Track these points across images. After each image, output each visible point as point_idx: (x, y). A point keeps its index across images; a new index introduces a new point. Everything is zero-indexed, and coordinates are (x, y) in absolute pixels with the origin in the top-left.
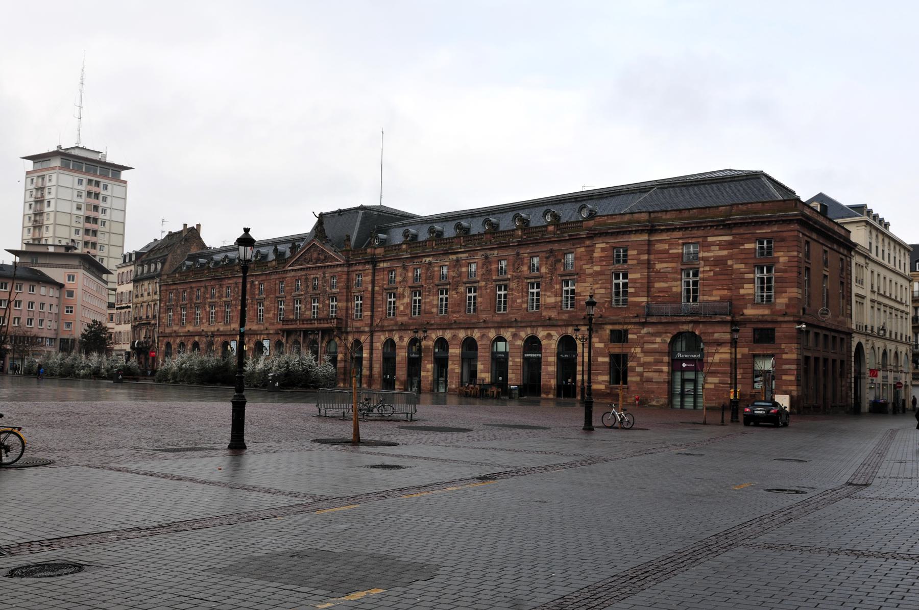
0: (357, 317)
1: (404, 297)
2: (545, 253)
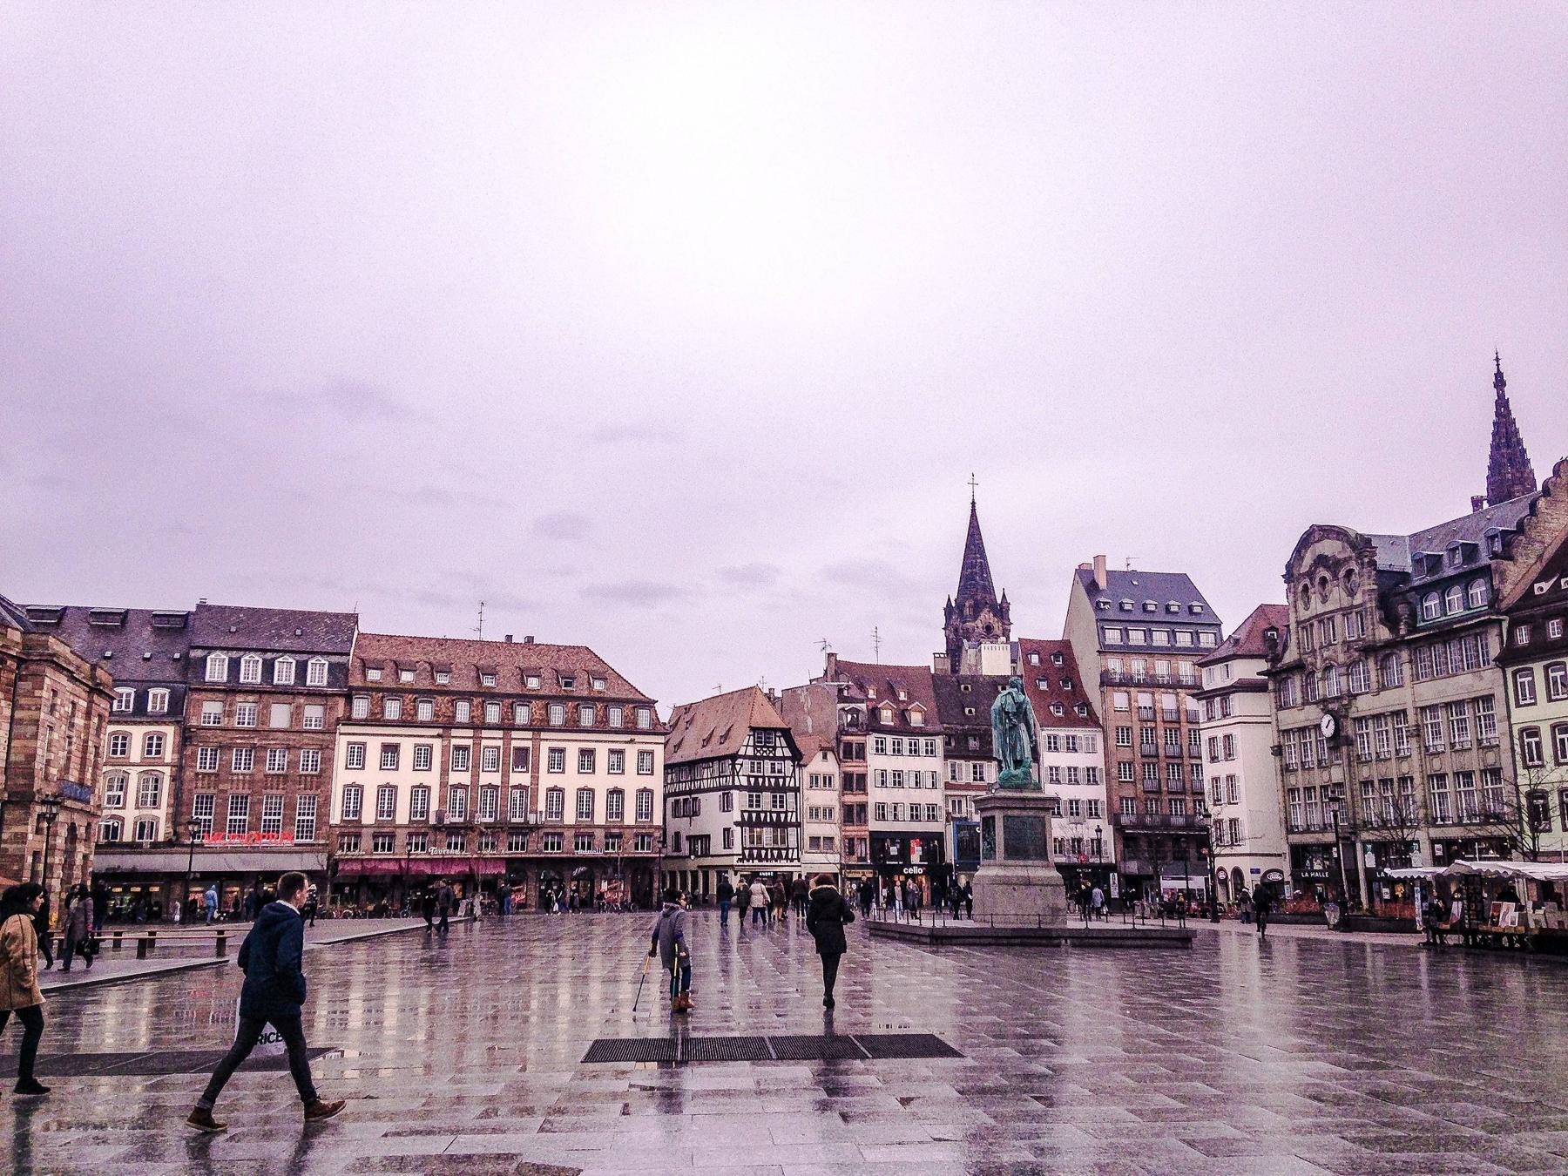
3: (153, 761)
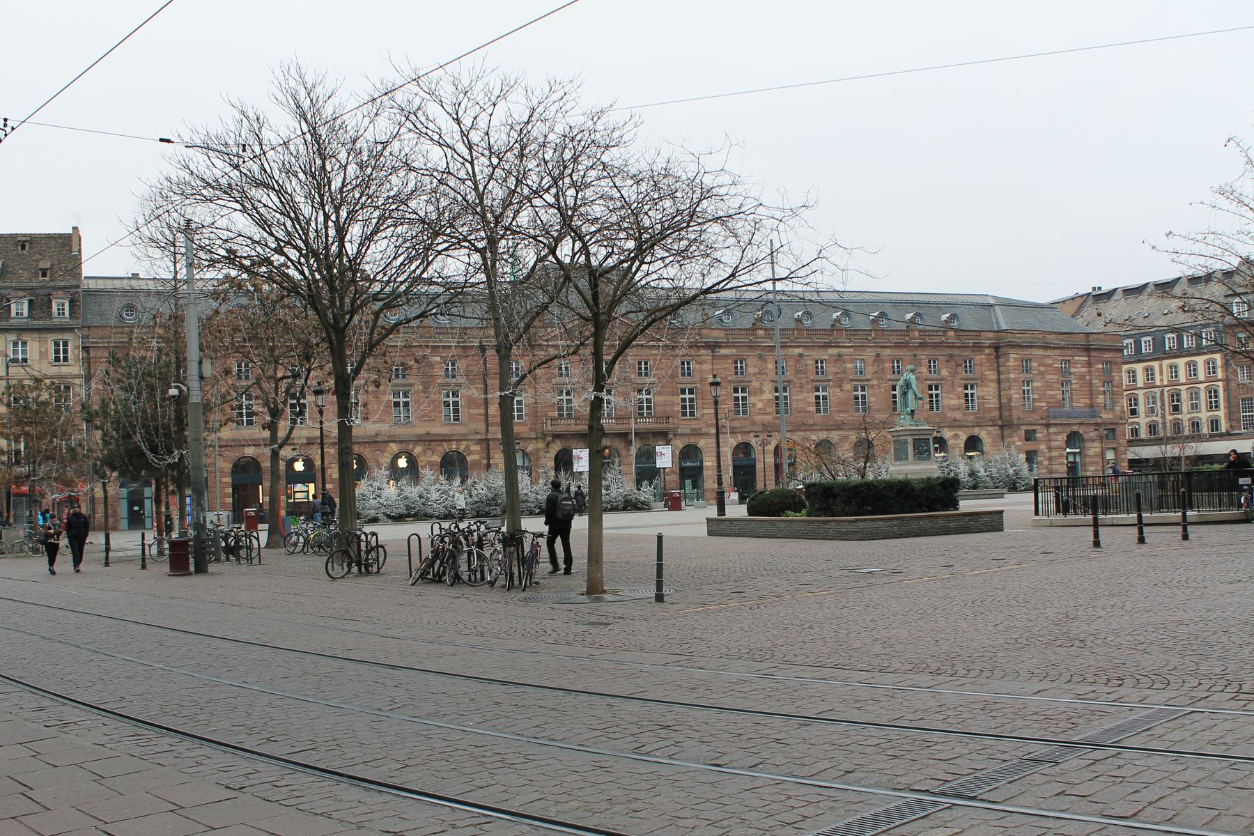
0: (684, 414)
1: (762, 392)
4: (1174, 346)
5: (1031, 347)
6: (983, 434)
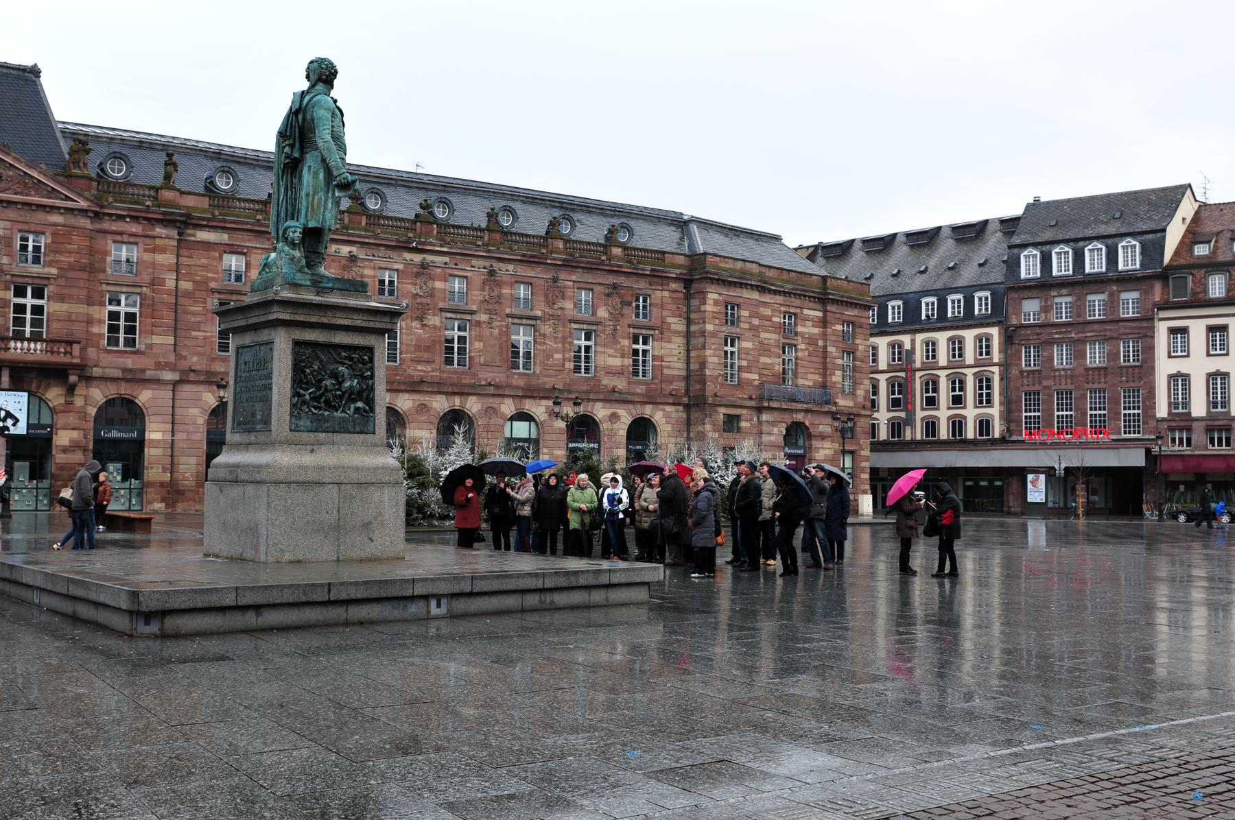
0: (113, 341)
2: (602, 287)
3: (959, 363)
4: (933, 315)
5: (741, 285)
6: (658, 416)
